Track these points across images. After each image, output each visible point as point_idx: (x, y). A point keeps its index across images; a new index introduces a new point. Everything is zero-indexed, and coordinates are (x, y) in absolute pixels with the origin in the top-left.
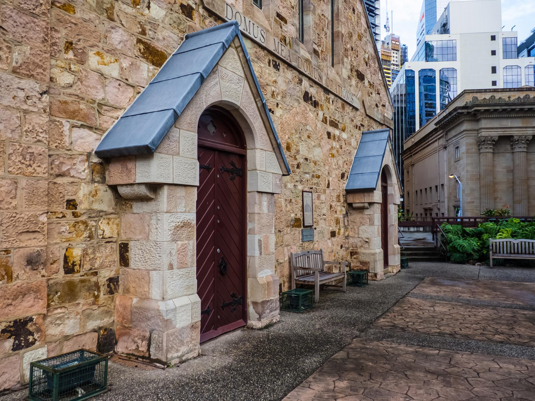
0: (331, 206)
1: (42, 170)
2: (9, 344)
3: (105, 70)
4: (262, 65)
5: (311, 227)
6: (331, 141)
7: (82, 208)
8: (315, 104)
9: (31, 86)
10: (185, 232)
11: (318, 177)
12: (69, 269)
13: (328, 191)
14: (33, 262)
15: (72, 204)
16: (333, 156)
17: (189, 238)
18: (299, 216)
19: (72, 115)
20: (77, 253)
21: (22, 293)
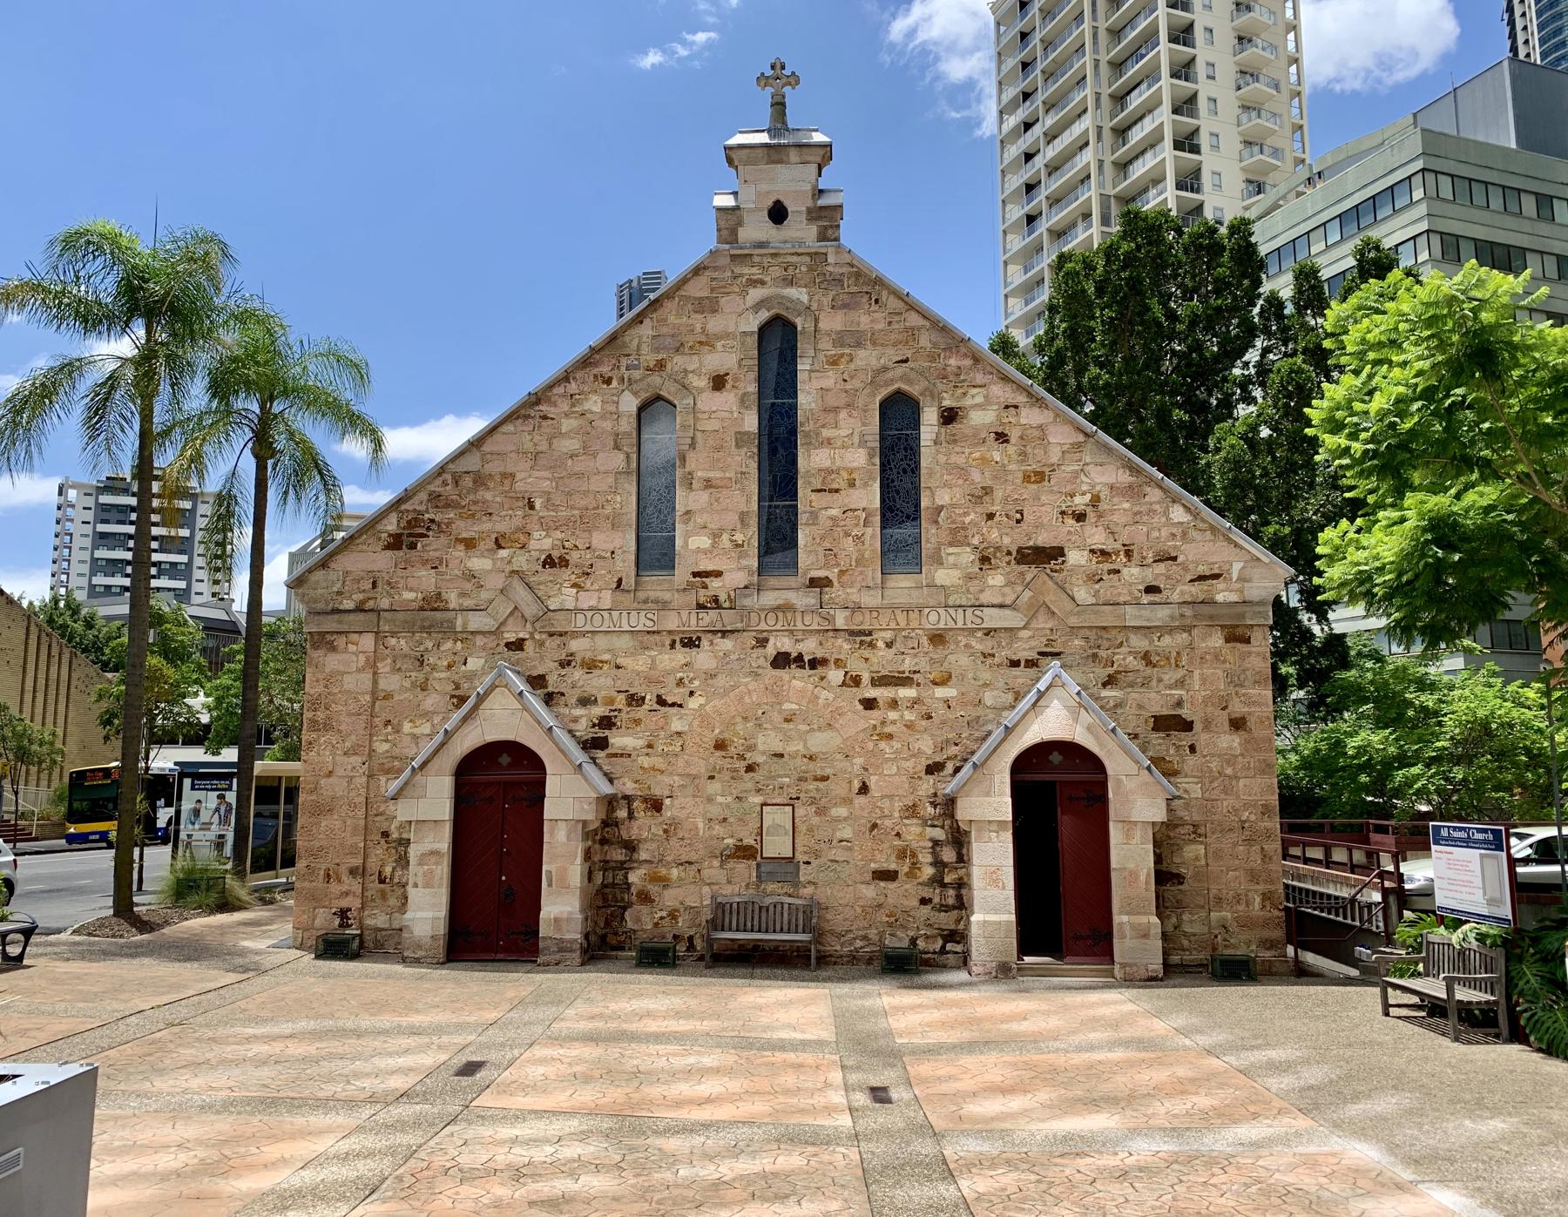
0: (875, 826)
1: (361, 813)
2: (337, 921)
3: (417, 731)
4: (653, 653)
5: (791, 860)
6: (874, 713)
7: (395, 836)
8: (814, 664)
9: (356, 760)
10: (433, 859)
11: (825, 779)
12: (382, 881)
13: (861, 800)
14: (353, 872)
15: (385, 834)
16: (890, 737)
17: (437, 864)
18: (749, 841)
19: (388, 772)
20: (388, 870)
21: (347, 894)
